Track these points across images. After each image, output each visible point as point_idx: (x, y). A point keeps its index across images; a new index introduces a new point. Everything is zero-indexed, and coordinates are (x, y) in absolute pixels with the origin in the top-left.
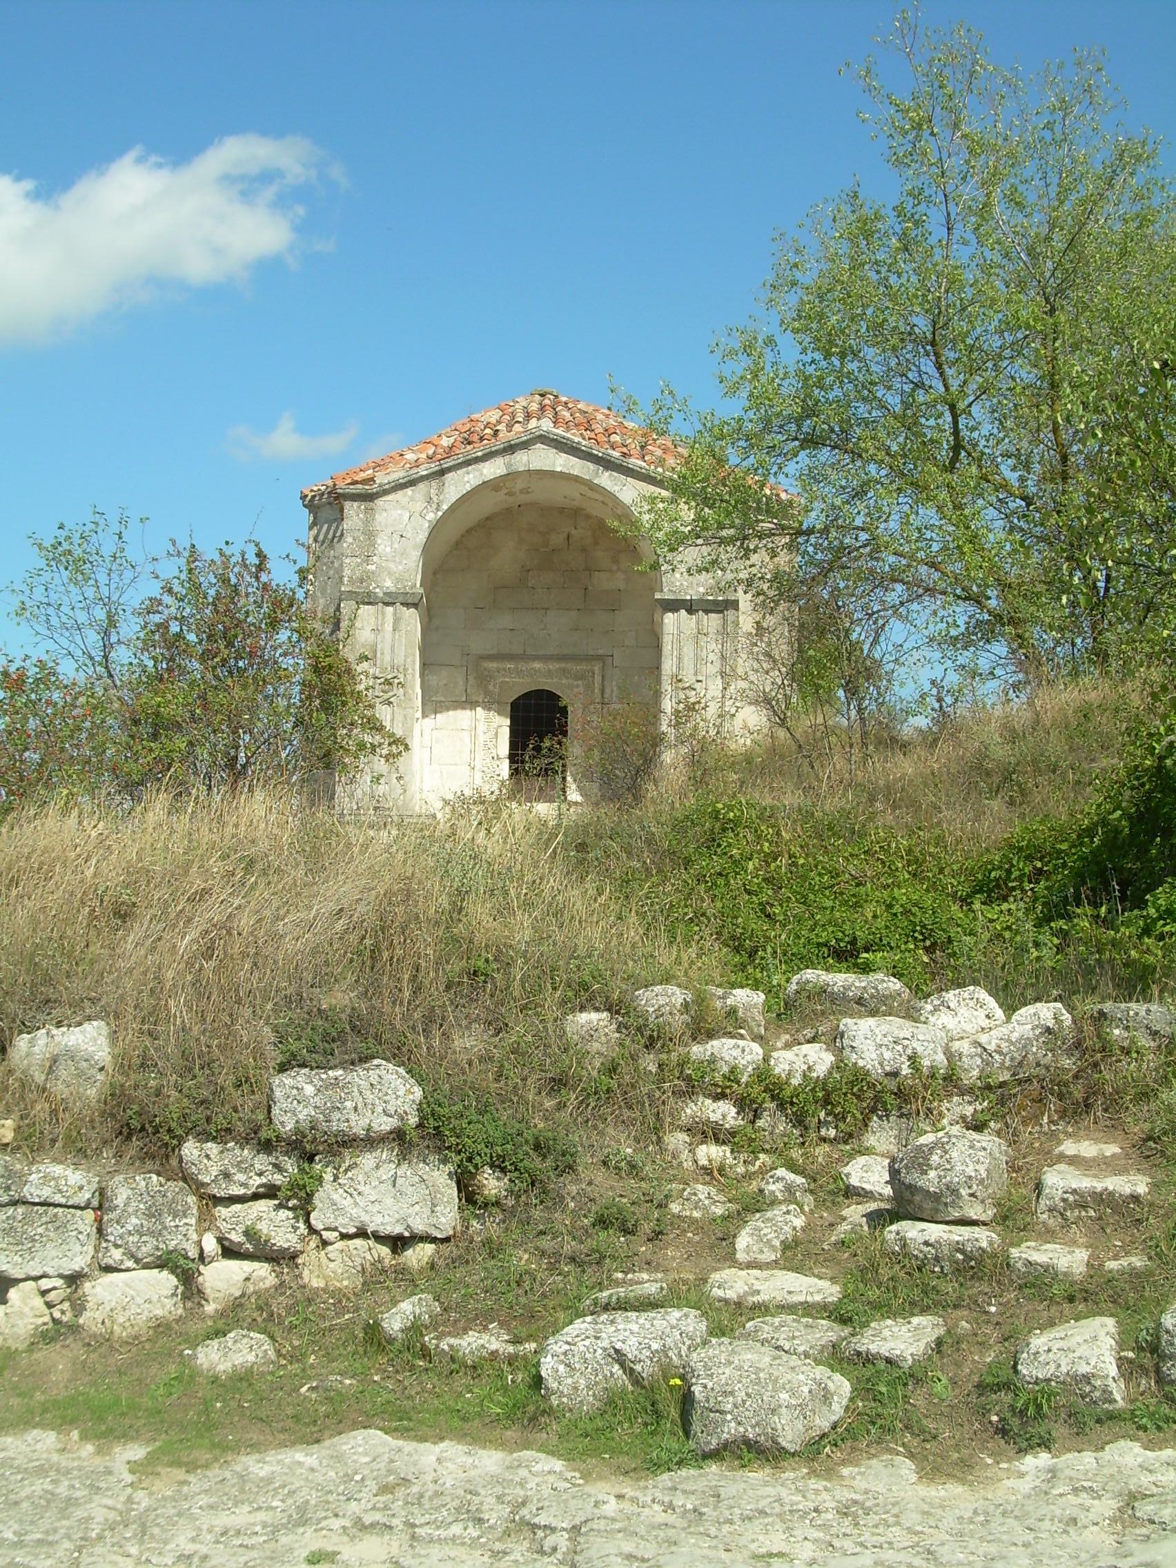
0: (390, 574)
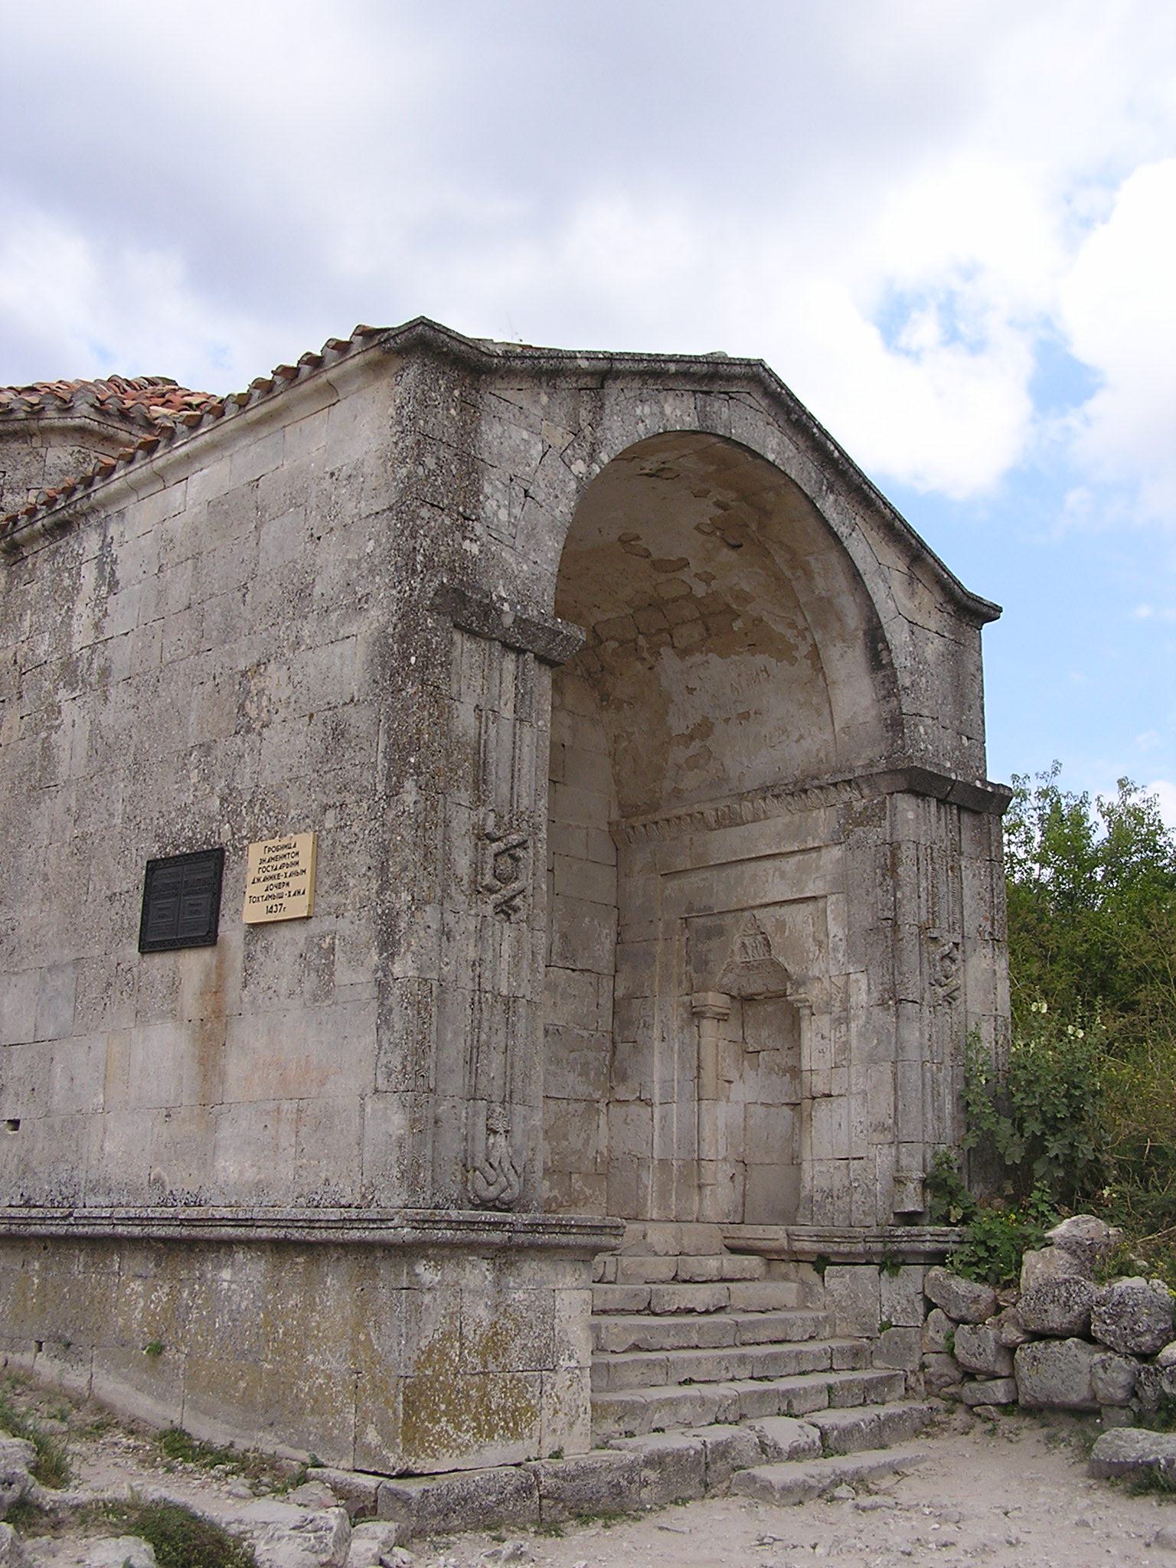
0: (509, 577)
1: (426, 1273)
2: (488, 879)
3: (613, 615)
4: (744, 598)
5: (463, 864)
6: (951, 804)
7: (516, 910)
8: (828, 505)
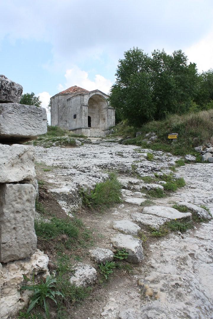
1: (83, 129)
5: (84, 115)
8: (103, 96)
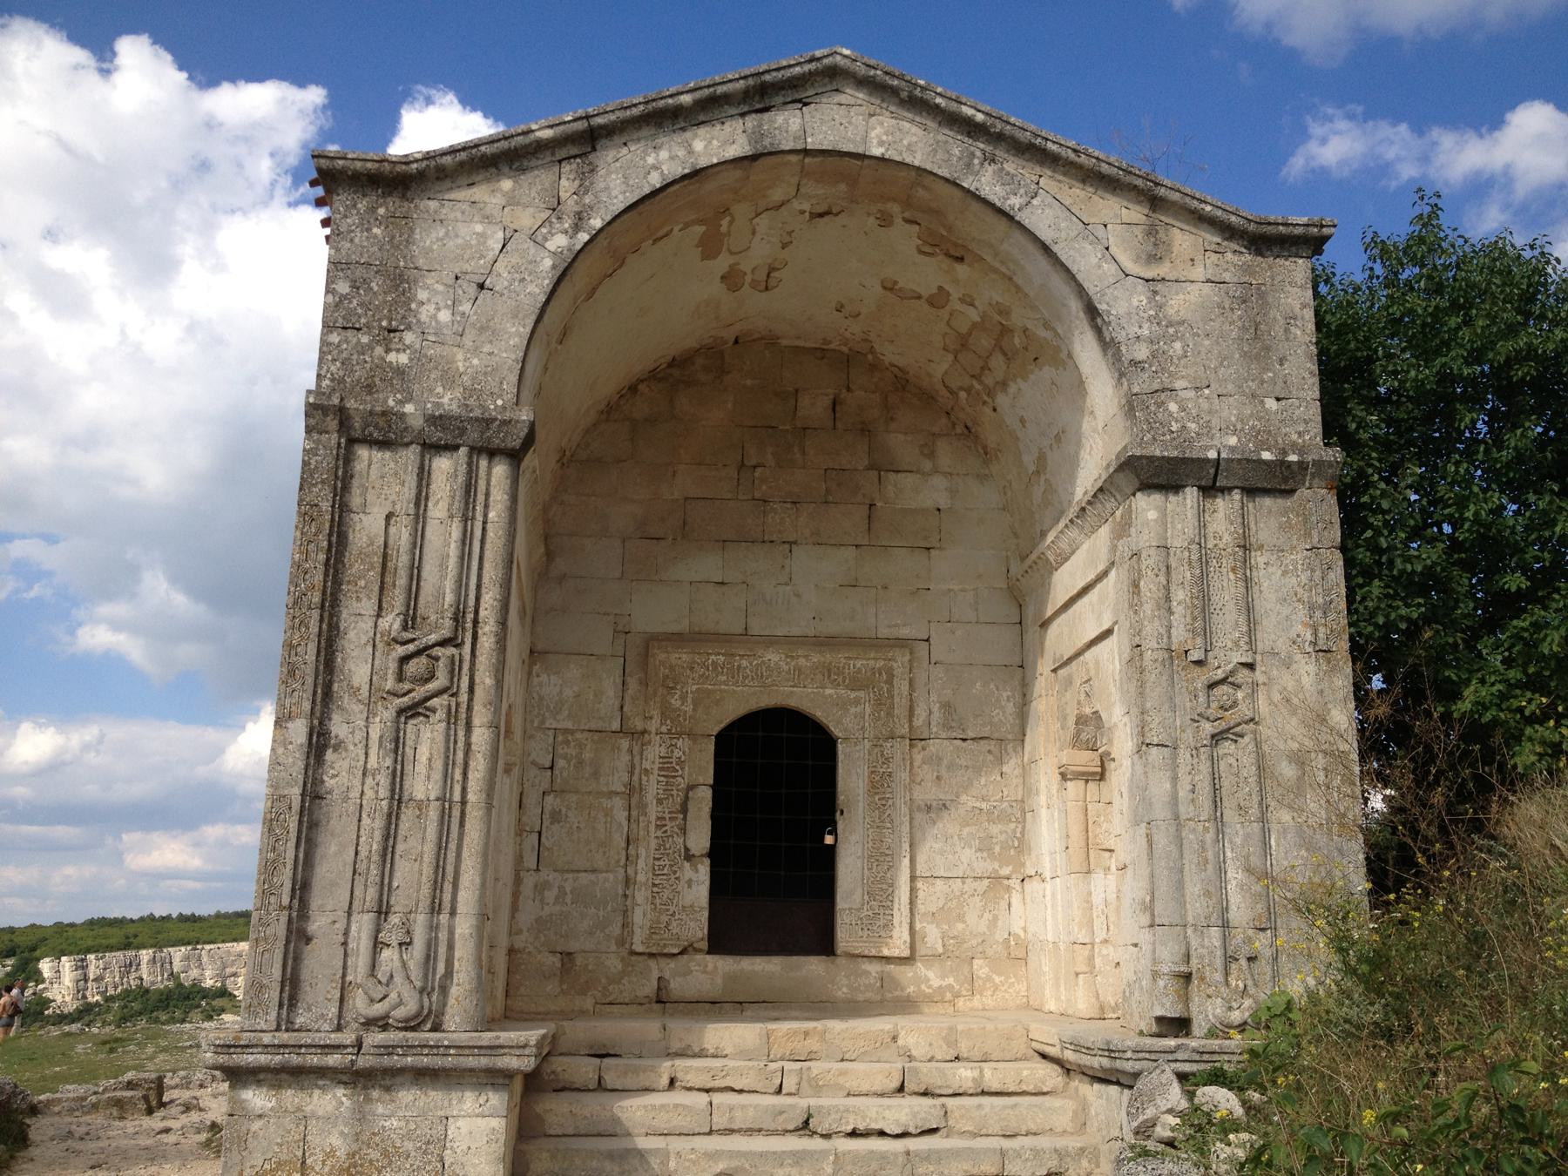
0: (449, 379)
2: (390, 684)
3: (945, 366)
4: (1004, 311)
6: (1230, 489)
7: (434, 711)
8: (987, 183)
